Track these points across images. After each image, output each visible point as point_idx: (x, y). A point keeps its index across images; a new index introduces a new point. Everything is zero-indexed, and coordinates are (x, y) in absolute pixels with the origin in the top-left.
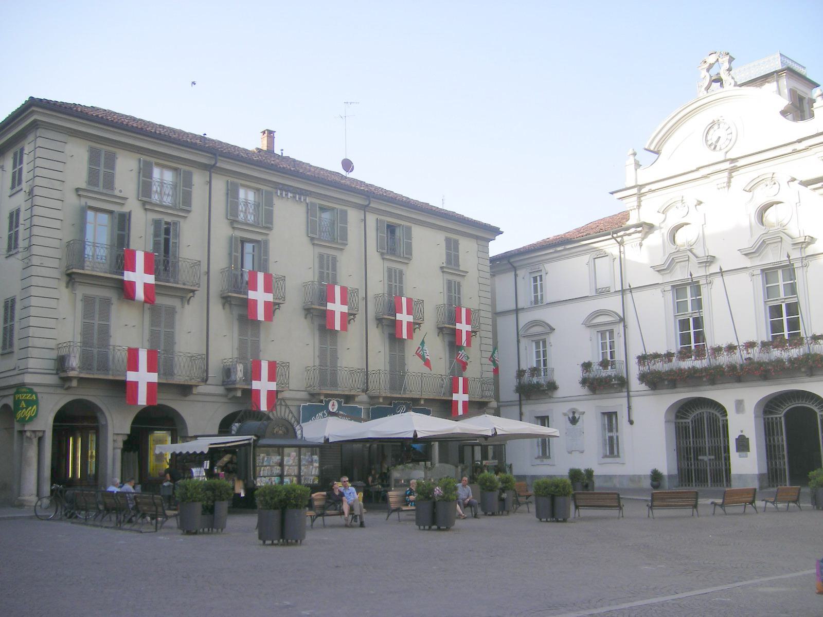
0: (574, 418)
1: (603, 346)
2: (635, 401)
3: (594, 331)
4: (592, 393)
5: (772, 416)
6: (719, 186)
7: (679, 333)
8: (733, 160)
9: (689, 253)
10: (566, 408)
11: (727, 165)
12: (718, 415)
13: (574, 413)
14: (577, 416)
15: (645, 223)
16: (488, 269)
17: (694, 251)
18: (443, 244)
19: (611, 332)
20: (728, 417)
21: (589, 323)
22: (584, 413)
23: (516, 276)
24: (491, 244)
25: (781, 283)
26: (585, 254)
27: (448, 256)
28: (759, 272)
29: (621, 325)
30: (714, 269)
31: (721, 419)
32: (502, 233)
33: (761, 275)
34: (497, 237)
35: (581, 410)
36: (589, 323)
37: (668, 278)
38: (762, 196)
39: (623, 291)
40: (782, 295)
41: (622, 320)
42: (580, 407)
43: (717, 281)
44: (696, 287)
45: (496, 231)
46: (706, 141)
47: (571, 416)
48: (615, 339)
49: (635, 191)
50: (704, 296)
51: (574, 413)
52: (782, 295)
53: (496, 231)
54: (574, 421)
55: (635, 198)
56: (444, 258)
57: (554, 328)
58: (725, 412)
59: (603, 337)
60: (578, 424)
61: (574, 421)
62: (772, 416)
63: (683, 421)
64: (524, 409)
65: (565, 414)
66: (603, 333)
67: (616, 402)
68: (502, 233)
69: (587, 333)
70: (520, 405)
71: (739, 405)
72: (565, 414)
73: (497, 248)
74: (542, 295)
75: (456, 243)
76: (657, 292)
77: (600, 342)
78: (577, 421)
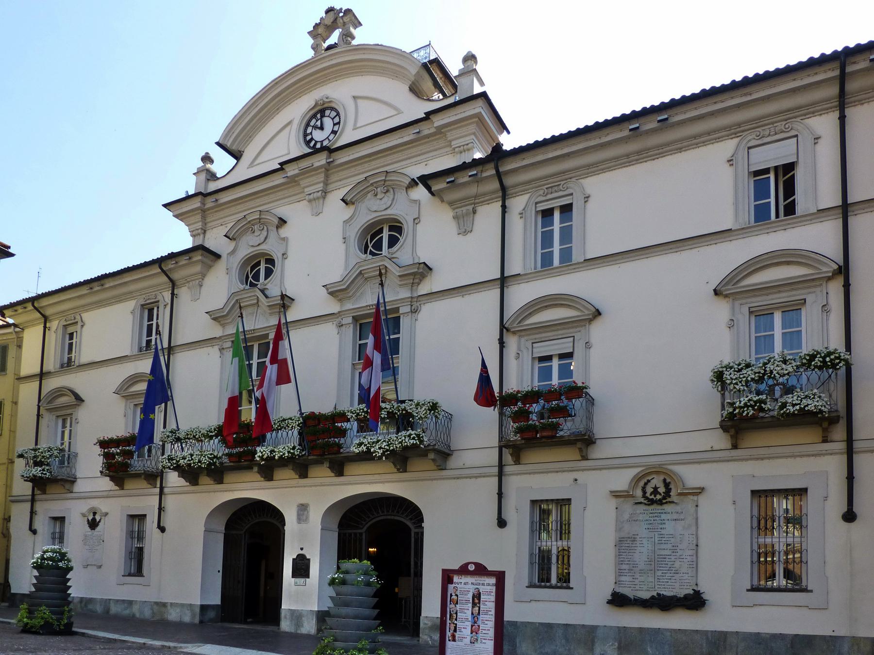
0: (94, 519)
2: (170, 502)
4: (117, 488)
5: (350, 531)
13: (95, 514)
14: (98, 518)
22: (106, 514)
35: (104, 510)
38: (372, 209)
42: (103, 506)
47: (90, 518)
51: (95, 514)
54: (93, 524)
61: (93, 524)
62: (350, 531)
64: (38, 506)
65: (84, 515)
67: (145, 501)
70: (33, 501)
72: (84, 515)
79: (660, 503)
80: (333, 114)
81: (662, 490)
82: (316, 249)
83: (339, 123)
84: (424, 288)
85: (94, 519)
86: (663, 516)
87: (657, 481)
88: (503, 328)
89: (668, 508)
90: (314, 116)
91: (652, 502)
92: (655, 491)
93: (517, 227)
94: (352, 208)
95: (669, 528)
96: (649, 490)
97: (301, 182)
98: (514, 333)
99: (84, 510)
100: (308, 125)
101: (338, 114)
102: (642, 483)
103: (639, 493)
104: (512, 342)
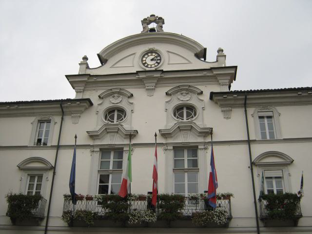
1: (31, 186)
7: (99, 184)
15: (89, 100)
21: (22, 168)
26: (34, 116)
28: (172, 148)
33: (172, 151)
36: (22, 168)
37: (98, 142)
39: (58, 147)
40: (186, 166)
41: (53, 168)
44: (119, 151)
46: (142, 61)
48: (43, 183)
52: (186, 166)
55: (84, 84)
66: (32, 177)
69: (19, 175)
77: (28, 183)
82: (150, 113)
83: (160, 60)
88: (253, 164)
93: (251, 120)
94: (168, 99)
97: (145, 82)
98: (256, 165)
101: (159, 56)
104: (255, 169)
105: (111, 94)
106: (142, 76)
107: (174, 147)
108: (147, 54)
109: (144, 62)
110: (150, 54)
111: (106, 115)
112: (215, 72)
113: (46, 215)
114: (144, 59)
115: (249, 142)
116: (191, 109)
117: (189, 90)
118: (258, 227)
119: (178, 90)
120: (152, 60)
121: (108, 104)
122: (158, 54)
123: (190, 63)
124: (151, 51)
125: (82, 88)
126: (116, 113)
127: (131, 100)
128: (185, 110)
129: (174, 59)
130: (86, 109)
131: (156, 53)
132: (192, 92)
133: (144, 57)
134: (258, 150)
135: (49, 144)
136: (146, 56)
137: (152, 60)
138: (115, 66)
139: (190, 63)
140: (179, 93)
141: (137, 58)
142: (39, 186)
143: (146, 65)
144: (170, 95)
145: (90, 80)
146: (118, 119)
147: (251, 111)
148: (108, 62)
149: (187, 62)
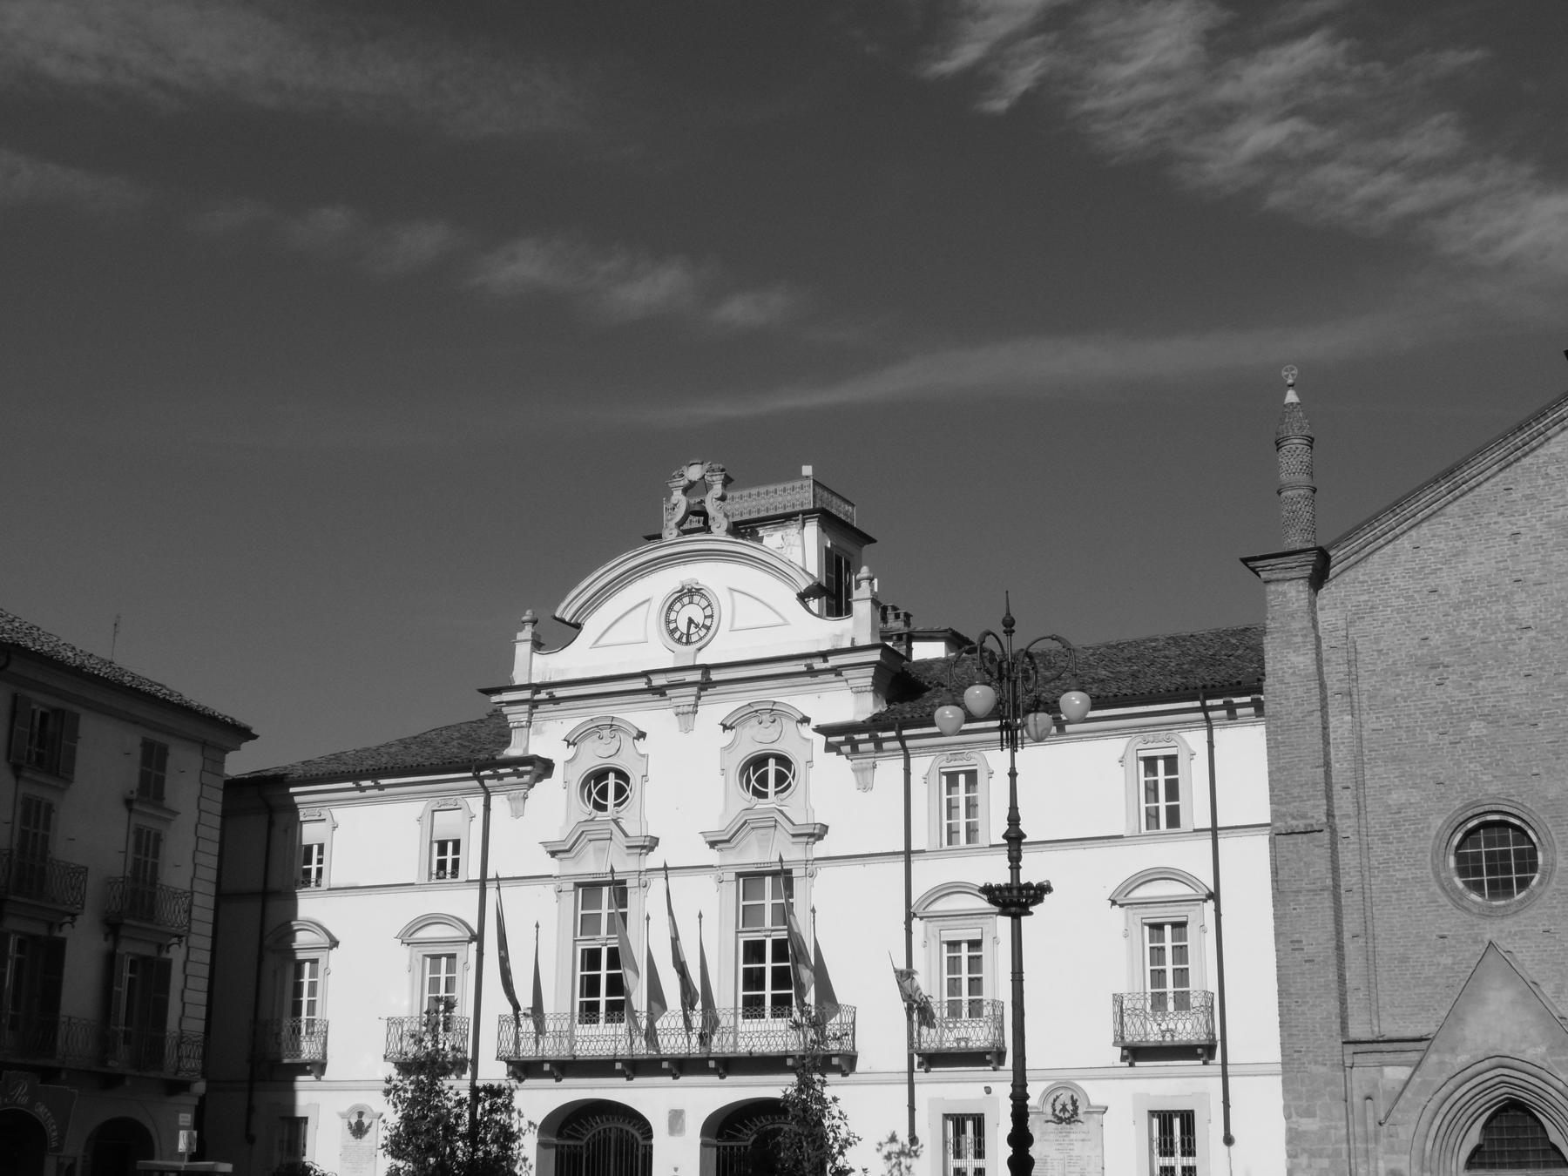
0: (360, 1124)
3: (419, 952)
6: (680, 710)
8: (706, 668)
9: (613, 826)
10: (348, 1101)
11: (696, 676)
12: (637, 1135)
13: (361, 1114)
14: (366, 1121)
16: (218, 808)
17: (623, 824)
18: (137, 753)
19: (452, 957)
20: (654, 1141)
21: (408, 937)
23: (271, 824)
24: (231, 757)
25: (768, 902)
27: (144, 777)
28: (733, 877)
29: (474, 945)
30: (654, 860)
31: (641, 1142)
32: (255, 737)
34: (244, 746)
36: (408, 937)
41: (478, 938)
43: (658, 883)
45: (244, 734)
46: (668, 622)
47: (354, 1120)
48: (458, 975)
49: (526, 695)
50: (632, 910)
51: (361, 1114)
53: (244, 734)
55: (526, 707)
56: (135, 782)
57: (337, 936)
58: (650, 1130)
59: (435, 969)
60: (367, 1137)
63: (571, 1142)
65: (343, 1116)
68: (255, 737)
71: (676, 1119)
72: (343, 1116)
73: (239, 763)
74: (319, 871)
75: (163, 752)
76: (549, 889)
78: (366, 1131)
79: (1069, 1121)
80: (704, 603)
81: (1070, 1107)
83: (711, 616)
84: (820, 849)
85: (360, 1124)
86: (1072, 1136)
87: (1065, 1098)
88: (910, 917)
89: (1075, 1127)
90: (679, 599)
91: (1060, 1120)
92: (1064, 1109)
95: (1077, 1149)
96: (1058, 1107)
99: (345, 1108)
100: (670, 608)
102: (1051, 1100)
103: (1049, 1110)
105: (595, 729)
106: (658, 681)
107: (739, 875)
108: (679, 599)
109: (672, 626)
110: (686, 600)
111: (590, 793)
112: (833, 661)
113: (470, 1056)
114: (673, 616)
115: (908, 854)
116: (783, 761)
117: (774, 712)
118: (911, 1071)
119: (753, 713)
120: (691, 621)
121: (594, 755)
122: (707, 599)
123: (786, 623)
124: (689, 593)
125: (524, 718)
126: (605, 786)
127: (640, 743)
128: (765, 772)
129: (749, 613)
130: (539, 778)
131: (703, 596)
132: (788, 716)
133: (670, 608)
134: (927, 875)
135: (462, 877)
136: (677, 606)
137: (691, 621)
138: (601, 642)
139: (786, 623)
140: (754, 721)
141: (652, 617)
142: (450, 984)
143: (677, 635)
144: (731, 728)
145: (537, 697)
146: (617, 798)
147: (921, 764)
148: (585, 628)
149: (781, 621)
